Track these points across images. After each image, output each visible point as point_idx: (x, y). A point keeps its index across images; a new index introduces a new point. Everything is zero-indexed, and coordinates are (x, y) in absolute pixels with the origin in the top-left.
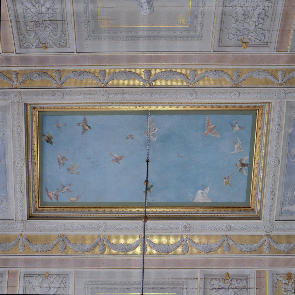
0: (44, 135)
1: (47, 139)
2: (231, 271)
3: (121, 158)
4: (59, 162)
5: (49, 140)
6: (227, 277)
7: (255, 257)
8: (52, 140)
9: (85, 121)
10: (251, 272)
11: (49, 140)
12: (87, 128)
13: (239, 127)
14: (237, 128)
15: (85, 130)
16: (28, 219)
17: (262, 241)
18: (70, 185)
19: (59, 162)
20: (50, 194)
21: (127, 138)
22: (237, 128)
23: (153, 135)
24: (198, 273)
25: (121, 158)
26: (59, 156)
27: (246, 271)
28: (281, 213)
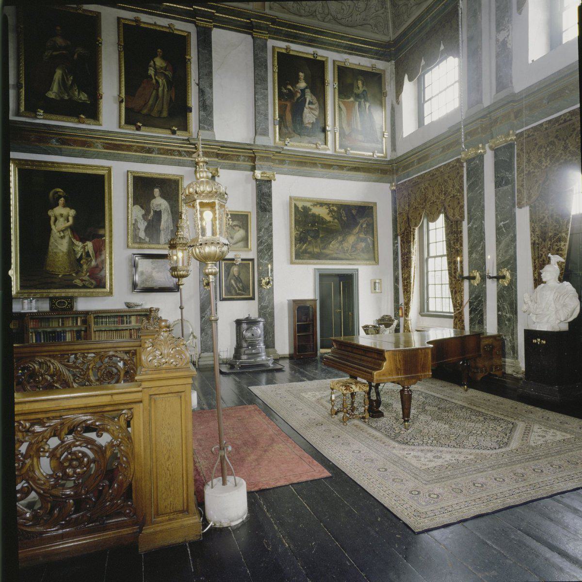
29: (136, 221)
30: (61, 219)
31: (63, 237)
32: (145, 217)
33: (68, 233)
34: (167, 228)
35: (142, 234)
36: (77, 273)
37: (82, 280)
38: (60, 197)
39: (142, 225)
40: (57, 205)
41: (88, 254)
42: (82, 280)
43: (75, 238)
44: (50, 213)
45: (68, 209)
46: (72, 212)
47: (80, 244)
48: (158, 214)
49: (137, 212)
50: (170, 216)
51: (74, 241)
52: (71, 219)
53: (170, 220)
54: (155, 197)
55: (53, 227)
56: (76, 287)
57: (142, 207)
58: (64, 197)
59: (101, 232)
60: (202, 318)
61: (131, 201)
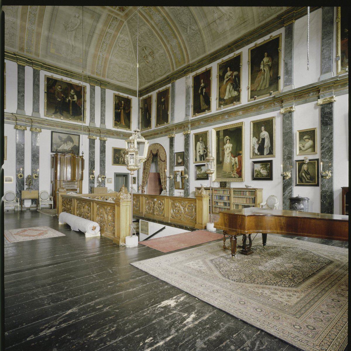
29: (254, 145)
30: (228, 149)
31: (228, 157)
32: (258, 142)
33: (230, 154)
34: (268, 146)
35: (256, 151)
36: (232, 172)
37: (234, 175)
38: (227, 139)
39: (257, 147)
40: (227, 143)
41: (236, 163)
42: (234, 175)
43: (232, 156)
44: (225, 147)
45: (230, 144)
46: (231, 145)
47: (233, 159)
48: (263, 140)
49: (255, 140)
50: (269, 140)
51: (232, 157)
52: (231, 148)
53: (269, 142)
54: (262, 131)
55: (225, 152)
56: (232, 177)
57: (256, 138)
58: (229, 139)
59: (240, 152)
60: (283, 195)
61: (252, 135)
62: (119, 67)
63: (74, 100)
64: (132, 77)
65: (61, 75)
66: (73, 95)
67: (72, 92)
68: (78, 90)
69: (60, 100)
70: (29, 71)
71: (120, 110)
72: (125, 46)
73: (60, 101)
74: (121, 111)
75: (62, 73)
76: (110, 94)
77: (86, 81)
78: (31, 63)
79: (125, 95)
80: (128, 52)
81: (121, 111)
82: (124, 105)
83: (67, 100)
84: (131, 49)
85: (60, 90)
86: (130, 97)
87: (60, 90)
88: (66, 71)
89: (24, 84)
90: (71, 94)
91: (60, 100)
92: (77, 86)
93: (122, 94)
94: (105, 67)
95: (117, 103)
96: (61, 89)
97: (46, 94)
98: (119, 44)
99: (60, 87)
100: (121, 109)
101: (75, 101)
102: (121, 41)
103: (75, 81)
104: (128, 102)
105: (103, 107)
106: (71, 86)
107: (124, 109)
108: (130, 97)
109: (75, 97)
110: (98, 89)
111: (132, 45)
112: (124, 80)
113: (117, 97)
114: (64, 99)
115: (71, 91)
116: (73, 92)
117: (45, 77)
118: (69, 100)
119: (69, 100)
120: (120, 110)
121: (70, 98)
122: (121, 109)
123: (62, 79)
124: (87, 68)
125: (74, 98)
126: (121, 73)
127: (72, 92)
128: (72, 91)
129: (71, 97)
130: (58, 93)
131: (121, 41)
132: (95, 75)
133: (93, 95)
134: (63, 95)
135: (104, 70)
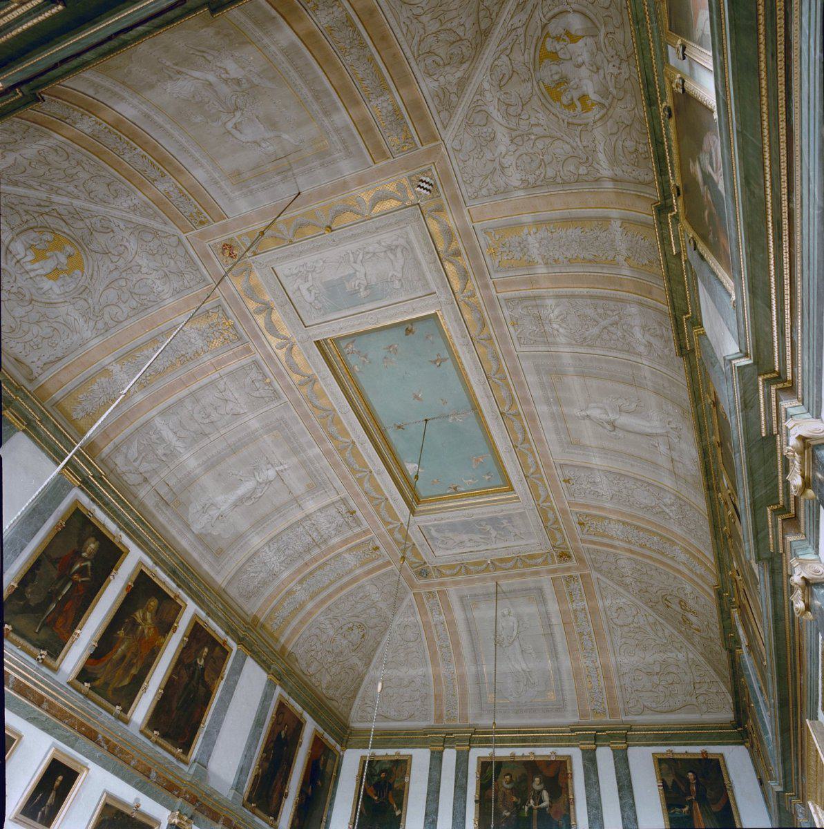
0: (412, 325)
1: (410, 329)
2: (358, 513)
3: (419, 399)
4: (390, 347)
5: (408, 331)
6: (352, 513)
7: (380, 524)
8: (411, 334)
9: (445, 360)
10: (366, 525)
11: (408, 331)
12: (438, 364)
13: (489, 479)
14: (487, 478)
15: (435, 362)
16: (315, 342)
17: (396, 522)
18: (370, 362)
19: (390, 347)
20: (351, 346)
21: (442, 400)
22: (487, 478)
23: (455, 419)
24: (344, 494)
25: (419, 399)
26: (396, 346)
27: (365, 522)
28: (425, 527)
62: (648, 674)
63: (544, 804)
64: (697, 686)
65: (513, 747)
66: (540, 792)
67: (537, 784)
68: (550, 773)
69: (508, 814)
70: (450, 756)
71: (686, 809)
72: (630, 619)
73: (510, 816)
74: (691, 810)
75: (512, 740)
76: (642, 761)
77: (568, 742)
78: (447, 741)
79: (696, 750)
80: (649, 628)
81: (691, 810)
82: (697, 784)
83: (526, 808)
84: (651, 619)
85: (506, 786)
86: (713, 750)
87: (508, 786)
88: (519, 732)
89: (438, 792)
90: (534, 790)
91: (508, 814)
92: (549, 763)
93: (679, 750)
94: (610, 688)
95: (669, 783)
96: (510, 782)
97: (478, 804)
98: (617, 622)
99: (508, 777)
100: (691, 802)
101: (544, 809)
102: (615, 615)
103: (543, 752)
104: (712, 770)
105: (627, 809)
106: (532, 767)
107: (701, 798)
108: (713, 750)
109: (545, 794)
110: (605, 756)
111: (646, 608)
112: (679, 705)
113: (663, 764)
114: (518, 808)
115: (533, 781)
116: (540, 783)
117: (478, 762)
118: (531, 809)
119: (531, 809)
120: (686, 809)
121: (532, 801)
122: (691, 802)
123: (513, 756)
124: (569, 708)
125: (541, 801)
126: (661, 688)
127: (537, 784)
128: (537, 779)
129: (533, 799)
130: (505, 795)
131: (615, 615)
132: (608, 719)
133: (593, 776)
134: (515, 799)
135: (611, 697)
